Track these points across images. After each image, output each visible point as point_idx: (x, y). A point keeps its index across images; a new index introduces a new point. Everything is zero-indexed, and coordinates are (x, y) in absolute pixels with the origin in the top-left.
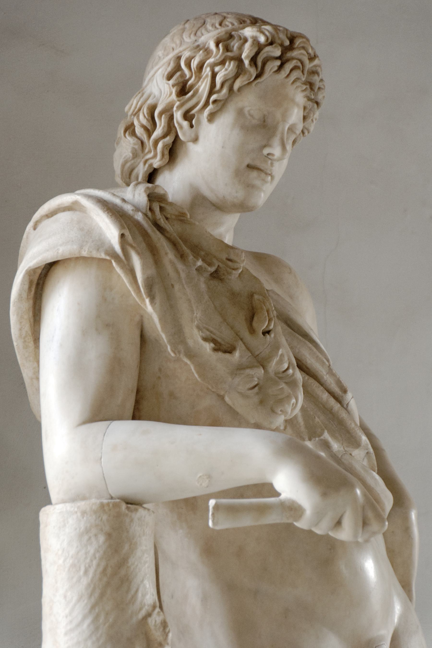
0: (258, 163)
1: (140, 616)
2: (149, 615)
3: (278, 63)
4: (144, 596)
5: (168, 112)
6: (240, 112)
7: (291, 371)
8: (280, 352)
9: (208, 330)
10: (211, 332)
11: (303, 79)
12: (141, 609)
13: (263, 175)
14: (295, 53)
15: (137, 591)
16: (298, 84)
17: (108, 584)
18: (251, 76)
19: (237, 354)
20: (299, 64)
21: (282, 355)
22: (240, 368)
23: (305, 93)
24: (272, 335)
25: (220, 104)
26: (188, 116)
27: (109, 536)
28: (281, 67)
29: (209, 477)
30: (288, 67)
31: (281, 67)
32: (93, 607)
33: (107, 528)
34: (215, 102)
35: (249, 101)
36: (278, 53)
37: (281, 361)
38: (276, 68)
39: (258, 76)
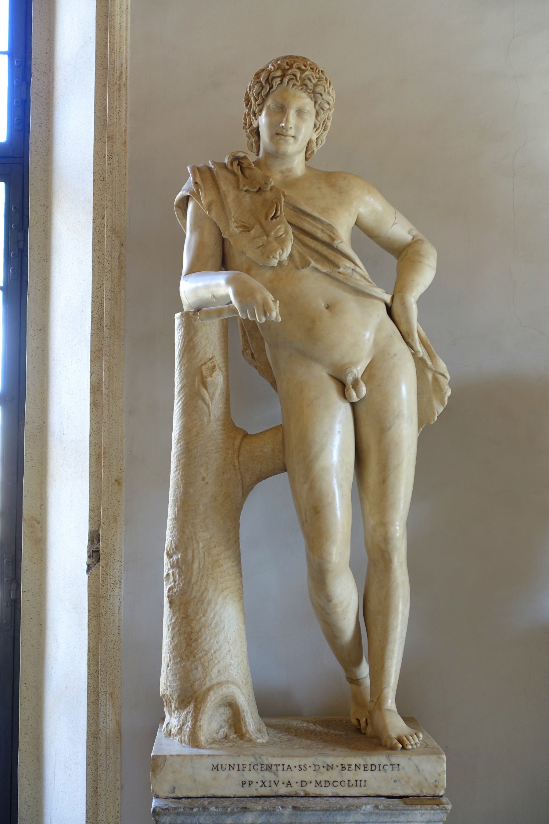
0: (279, 132)
1: (200, 364)
2: (205, 364)
3: (279, 79)
4: (205, 354)
5: (249, 114)
6: (269, 107)
7: (284, 236)
8: (279, 227)
9: (242, 222)
10: (244, 222)
11: (298, 84)
12: (201, 361)
13: (283, 137)
14: (289, 72)
15: (199, 352)
16: (295, 87)
17: (185, 350)
18: (267, 89)
19: (252, 232)
20: (292, 77)
21: (280, 228)
22: (254, 238)
23: (303, 90)
24: (278, 219)
25: (261, 106)
26: (255, 114)
27: (185, 328)
28: (282, 81)
29: (214, 296)
30: (286, 80)
31: (282, 81)
32: (180, 362)
33: (184, 325)
34: (259, 105)
35: (269, 102)
36: (279, 73)
37: (277, 232)
38: (279, 82)
39: (270, 89)
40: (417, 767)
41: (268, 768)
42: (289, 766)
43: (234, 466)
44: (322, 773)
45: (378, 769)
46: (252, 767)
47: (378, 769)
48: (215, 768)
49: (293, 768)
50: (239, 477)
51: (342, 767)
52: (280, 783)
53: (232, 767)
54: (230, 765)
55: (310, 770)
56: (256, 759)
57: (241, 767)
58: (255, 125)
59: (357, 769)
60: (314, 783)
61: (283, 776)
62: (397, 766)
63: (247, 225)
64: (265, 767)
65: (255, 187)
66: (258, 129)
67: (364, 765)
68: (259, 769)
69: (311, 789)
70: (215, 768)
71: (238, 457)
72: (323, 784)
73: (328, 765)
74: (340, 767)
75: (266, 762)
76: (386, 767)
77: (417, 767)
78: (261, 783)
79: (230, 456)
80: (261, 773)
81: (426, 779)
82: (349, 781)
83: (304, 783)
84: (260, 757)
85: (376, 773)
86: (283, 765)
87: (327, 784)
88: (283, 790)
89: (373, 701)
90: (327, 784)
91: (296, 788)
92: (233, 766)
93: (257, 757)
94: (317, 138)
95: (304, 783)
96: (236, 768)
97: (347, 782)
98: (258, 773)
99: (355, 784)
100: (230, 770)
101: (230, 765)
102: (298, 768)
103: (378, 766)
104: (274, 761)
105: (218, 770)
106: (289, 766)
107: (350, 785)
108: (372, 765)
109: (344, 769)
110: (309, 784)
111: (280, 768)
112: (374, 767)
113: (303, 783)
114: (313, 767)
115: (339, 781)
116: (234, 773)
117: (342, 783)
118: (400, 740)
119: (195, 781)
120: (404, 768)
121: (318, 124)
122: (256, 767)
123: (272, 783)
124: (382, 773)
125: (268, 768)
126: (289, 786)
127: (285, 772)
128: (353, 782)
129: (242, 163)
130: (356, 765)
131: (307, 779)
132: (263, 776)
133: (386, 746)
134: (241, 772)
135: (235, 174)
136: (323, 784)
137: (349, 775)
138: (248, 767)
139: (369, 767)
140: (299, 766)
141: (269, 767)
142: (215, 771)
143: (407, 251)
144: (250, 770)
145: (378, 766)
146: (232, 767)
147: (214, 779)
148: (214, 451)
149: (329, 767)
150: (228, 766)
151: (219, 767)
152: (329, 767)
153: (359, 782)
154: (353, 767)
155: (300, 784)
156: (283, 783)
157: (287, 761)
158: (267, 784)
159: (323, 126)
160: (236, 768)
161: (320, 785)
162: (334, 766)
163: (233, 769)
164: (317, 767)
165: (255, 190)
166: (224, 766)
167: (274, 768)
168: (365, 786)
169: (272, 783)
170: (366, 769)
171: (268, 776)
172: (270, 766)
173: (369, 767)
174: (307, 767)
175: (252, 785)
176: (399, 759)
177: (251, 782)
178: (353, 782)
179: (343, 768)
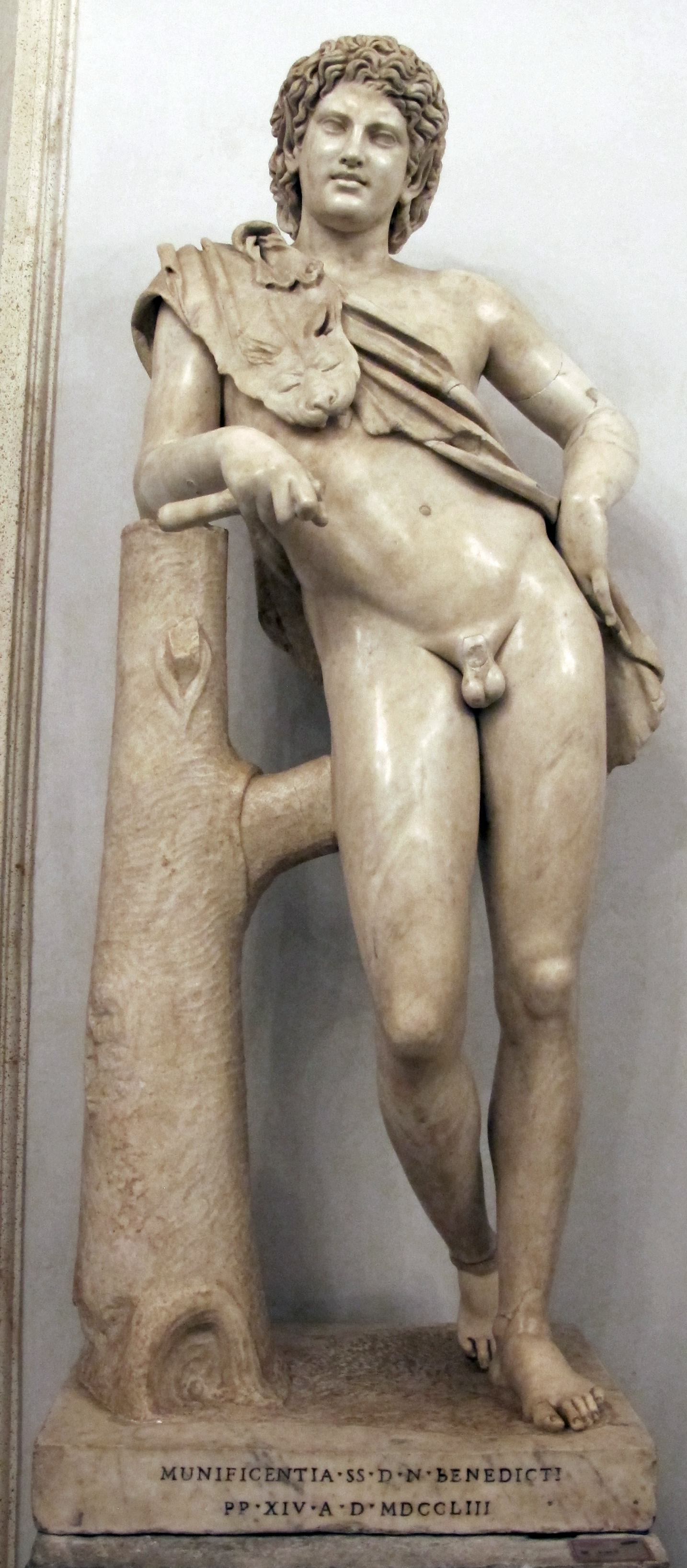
40: (597, 1473)
41: (282, 1474)
42: (327, 1471)
43: (231, 837)
44: (397, 1489)
45: (514, 1478)
46: (248, 1474)
47: (514, 1478)
48: (168, 1474)
49: (334, 1475)
50: (241, 859)
51: (440, 1475)
52: (307, 1509)
53: (204, 1473)
54: (201, 1470)
55: (372, 1481)
56: (257, 1459)
57: (224, 1473)
58: (291, 167)
59: (471, 1478)
60: (378, 1507)
61: (314, 1491)
62: (555, 1471)
63: (269, 349)
64: (275, 1475)
65: (286, 280)
66: (296, 176)
67: (486, 1470)
68: (263, 1478)
69: (373, 1520)
70: (168, 1474)
71: (239, 818)
72: (398, 1509)
73: (410, 1471)
74: (435, 1475)
75: (277, 1464)
76: (532, 1475)
77: (597, 1473)
78: (265, 1508)
79: (223, 816)
80: (267, 1487)
81: (616, 1499)
82: (453, 1503)
83: (357, 1509)
84: (265, 1455)
85: (511, 1486)
86: (314, 1470)
87: (407, 1510)
88: (312, 1521)
89: (504, 1316)
90: (407, 1510)
91: (340, 1517)
92: (206, 1471)
93: (259, 1452)
94: (414, 201)
95: (357, 1509)
96: (214, 1475)
97: (449, 1506)
98: (261, 1486)
99: (465, 1511)
100: (200, 1479)
101: (201, 1470)
102: (345, 1476)
103: (514, 1472)
104: (296, 1462)
105: (174, 1479)
106: (327, 1471)
107: (456, 1510)
108: (502, 1470)
109: (443, 1478)
110: (368, 1510)
111: (308, 1476)
112: (506, 1475)
113: (357, 1507)
114: (377, 1475)
115: (433, 1501)
116: (208, 1486)
117: (439, 1508)
118: (560, 1411)
119: (125, 1500)
120: (569, 1476)
121: (415, 167)
122: (256, 1474)
123: (290, 1507)
124: (525, 1488)
125: (282, 1474)
126: (326, 1513)
127: (318, 1484)
128: (461, 1505)
129: (265, 241)
130: (469, 1471)
131: (366, 1499)
132: (271, 1494)
133: (530, 1420)
134: (222, 1485)
135: (249, 259)
136: (398, 1509)
137: (452, 1492)
138: (239, 1473)
139: (496, 1475)
140: (349, 1472)
141: (284, 1475)
142: (169, 1481)
143: (585, 426)
144: (243, 1479)
145: (514, 1472)
146: (204, 1473)
147: (166, 1497)
148: (189, 805)
149: (412, 1475)
150: (196, 1472)
151: (178, 1473)
152: (412, 1475)
153: (473, 1507)
154: (463, 1474)
155: (349, 1510)
156: (313, 1508)
157: (322, 1464)
158: (279, 1508)
159: (423, 177)
160: (214, 1475)
161: (391, 1511)
162: (423, 1473)
163: (208, 1477)
164: (386, 1475)
165: (287, 284)
166: (187, 1471)
167: (295, 1476)
168: (486, 1513)
169: (290, 1507)
170: (490, 1478)
171: (282, 1492)
172: (287, 1472)
173: (496, 1475)
174: (366, 1474)
175: (247, 1512)
176: (559, 1448)
177: (244, 1506)
178: (461, 1505)
179: (441, 1475)
